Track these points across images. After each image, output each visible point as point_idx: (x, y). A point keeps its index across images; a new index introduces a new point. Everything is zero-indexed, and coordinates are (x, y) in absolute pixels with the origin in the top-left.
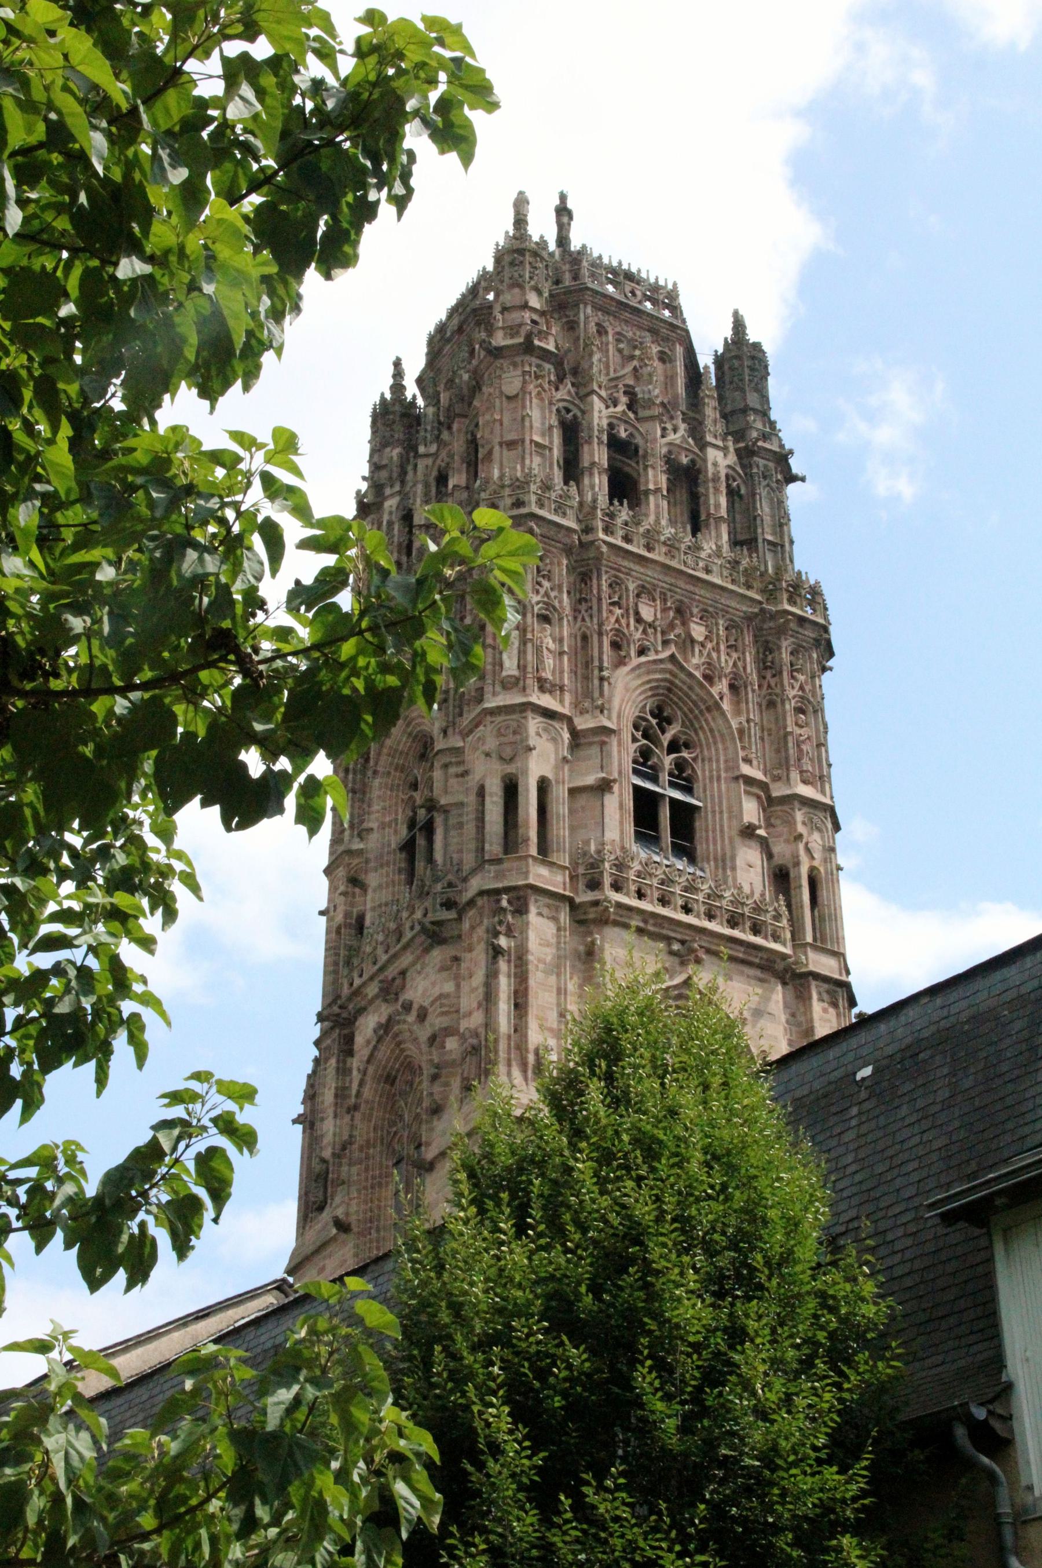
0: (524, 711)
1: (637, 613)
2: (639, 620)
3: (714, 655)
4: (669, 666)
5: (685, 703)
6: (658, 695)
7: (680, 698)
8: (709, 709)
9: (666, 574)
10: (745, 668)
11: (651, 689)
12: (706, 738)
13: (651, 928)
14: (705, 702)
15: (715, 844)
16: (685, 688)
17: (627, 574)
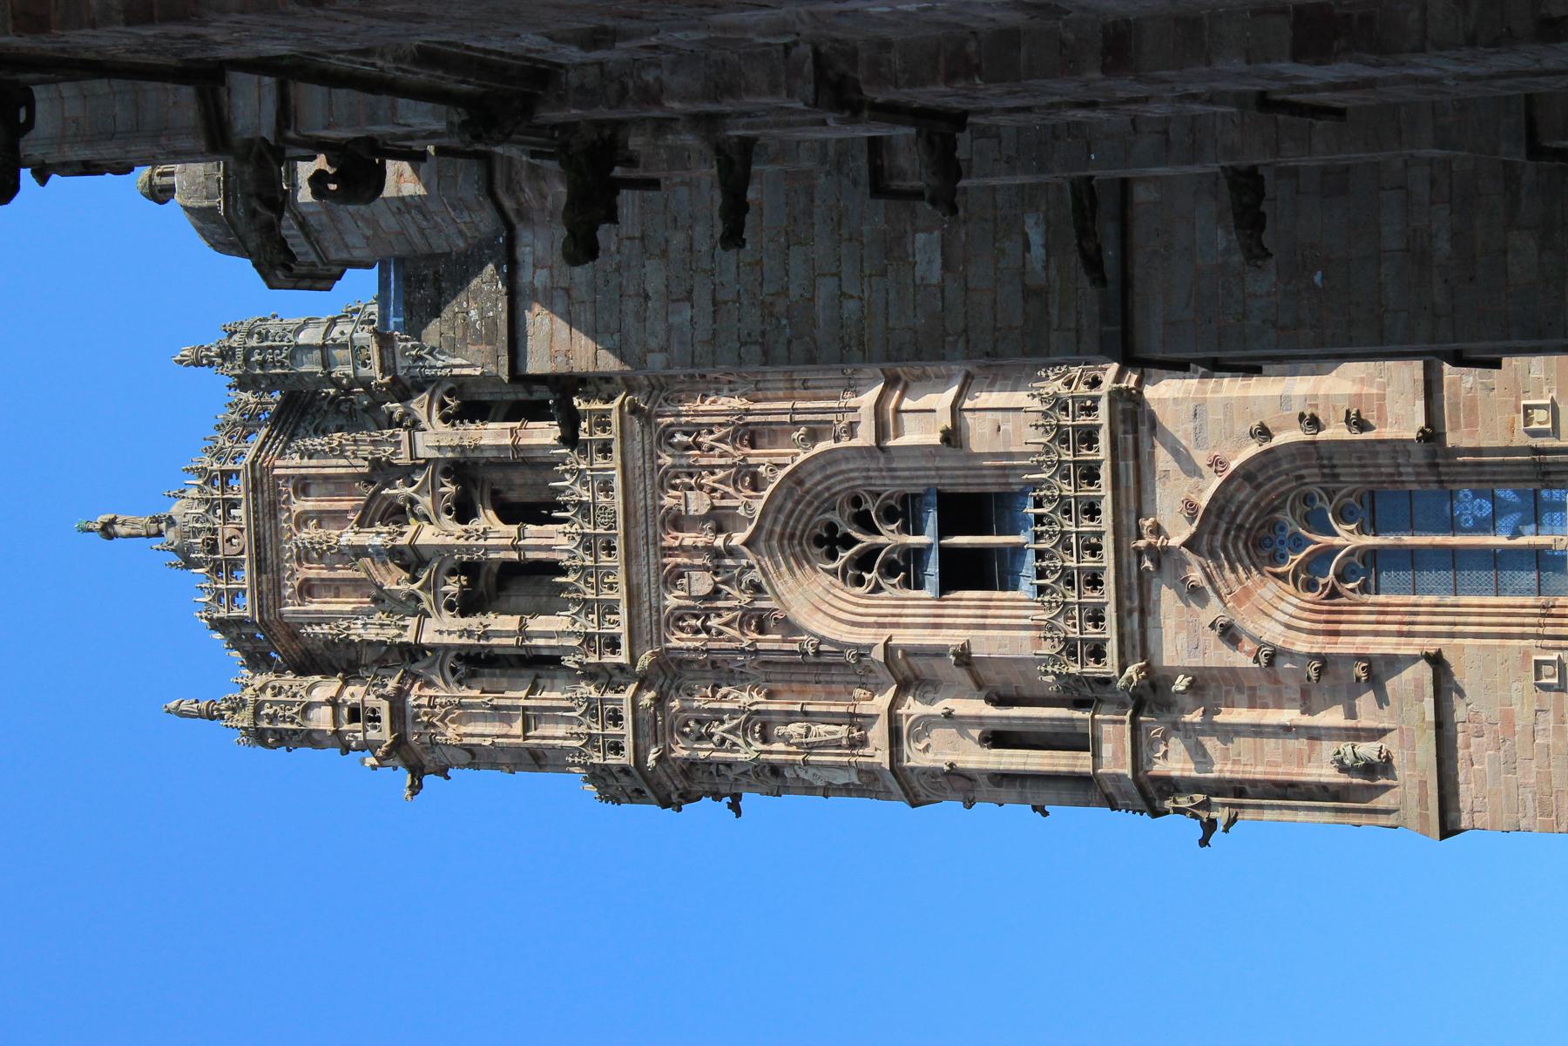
0: (903, 769)
1: (706, 598)
2: (716, 593)
3: (721, 474)
4: (762, 545)
5: (803, 512)
6: (803, 551)
7: (798, 521)
8: (800, 483)
9: (638, 556)
10: (720, 425)
11: (800, 566)
12: (841, 482)
13: (1136, 603)
14: (790, 491)
15: (985, 476)
16: (782, 518)
17: (658, 610)
